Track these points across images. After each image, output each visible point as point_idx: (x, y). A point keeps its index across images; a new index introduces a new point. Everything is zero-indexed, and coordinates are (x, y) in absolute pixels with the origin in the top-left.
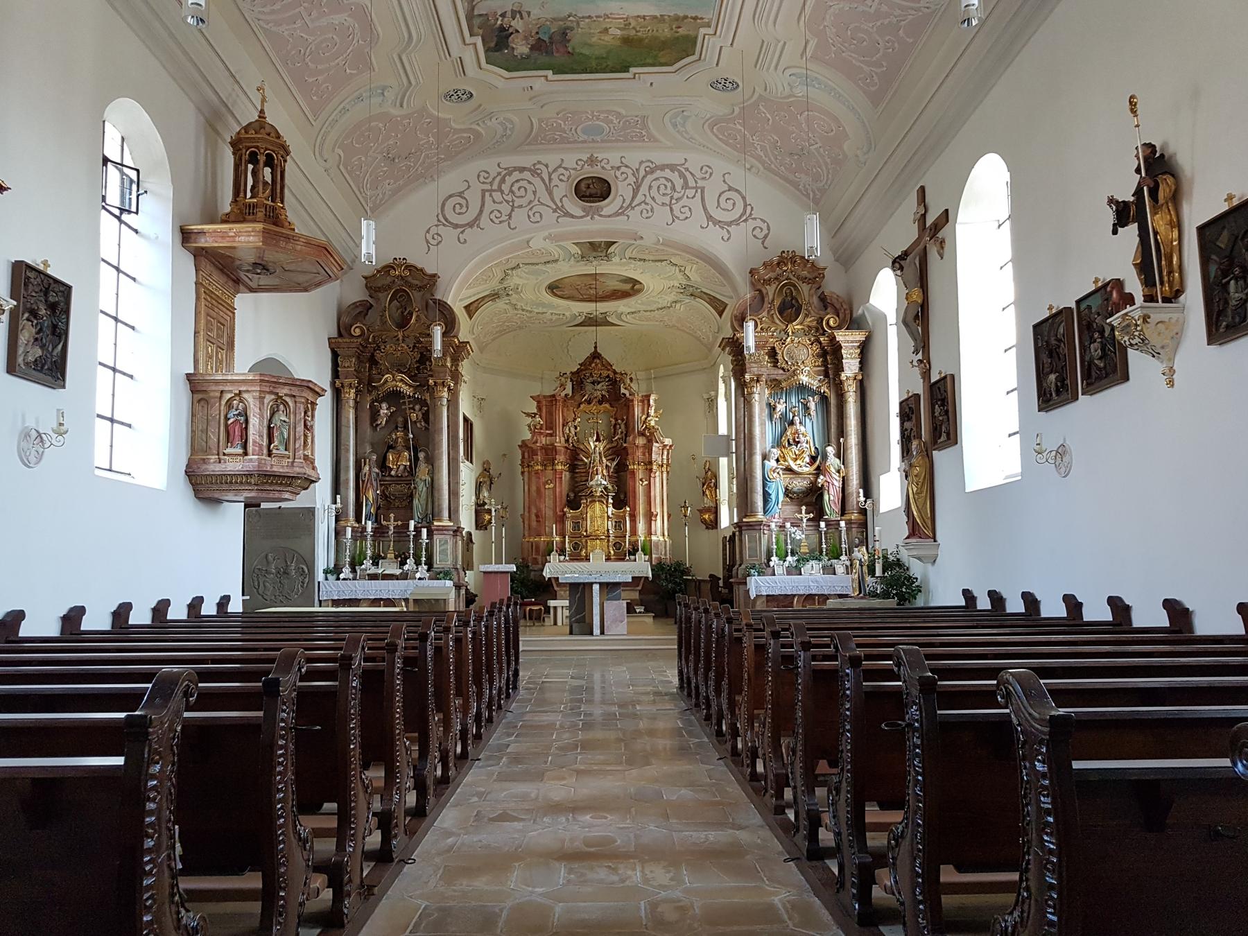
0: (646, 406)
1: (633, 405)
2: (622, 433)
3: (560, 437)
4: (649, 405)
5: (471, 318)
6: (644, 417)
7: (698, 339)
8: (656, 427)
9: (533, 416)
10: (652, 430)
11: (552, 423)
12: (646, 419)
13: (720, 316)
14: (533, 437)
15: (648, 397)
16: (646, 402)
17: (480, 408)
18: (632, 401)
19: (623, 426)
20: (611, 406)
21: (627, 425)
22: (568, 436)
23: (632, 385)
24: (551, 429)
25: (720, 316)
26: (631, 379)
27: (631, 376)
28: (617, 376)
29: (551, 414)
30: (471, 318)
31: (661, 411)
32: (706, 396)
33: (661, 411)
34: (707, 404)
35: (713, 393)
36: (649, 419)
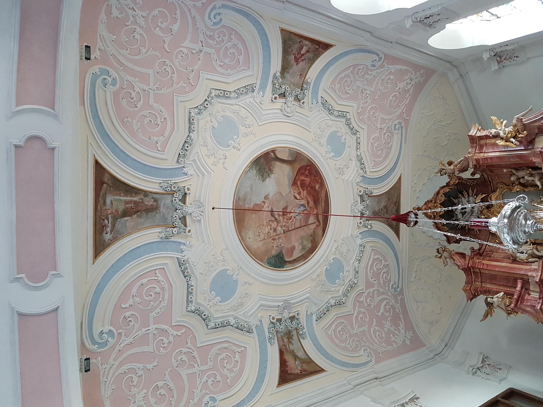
0: (488, 141)
1: (486, 159)
2: (531, 175)
3: (530, 270)
4: (487, 137)
5: (322, 370)
6: (500, 142)
7: (419, 87)
8: (514, 121)
9: (490, 305)
10: (519, 127)
11: (507, 279)
12: (502, 139)
13: (327, 46)
14: (524, 311)
15: (473, 140)
16: (482, 142)
17: (497, 367)
18: (477, 160)
19: (521, 174)
20: (494, 191)
21: (518, 167)
22: (533, 256)
23: (456, 163)
24: (515, 281)
25: (327, 46)
26: (450, 163)
27: (445, 163)
28: (452, 183)
29: (493, 278)
30: (322, 370)
31: (494, 118)
32: (495, 66)
33: (494, 118)
34: (507, 63)
35: (486, 56)
36: (502, 134)
